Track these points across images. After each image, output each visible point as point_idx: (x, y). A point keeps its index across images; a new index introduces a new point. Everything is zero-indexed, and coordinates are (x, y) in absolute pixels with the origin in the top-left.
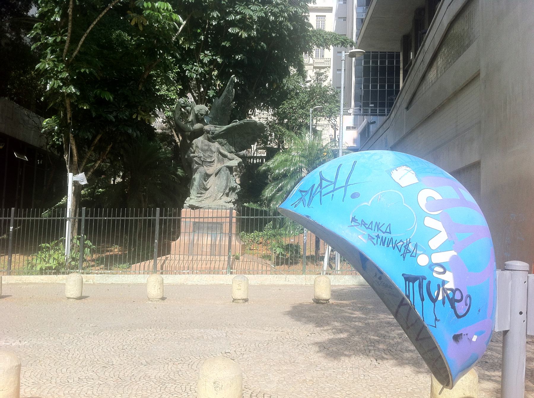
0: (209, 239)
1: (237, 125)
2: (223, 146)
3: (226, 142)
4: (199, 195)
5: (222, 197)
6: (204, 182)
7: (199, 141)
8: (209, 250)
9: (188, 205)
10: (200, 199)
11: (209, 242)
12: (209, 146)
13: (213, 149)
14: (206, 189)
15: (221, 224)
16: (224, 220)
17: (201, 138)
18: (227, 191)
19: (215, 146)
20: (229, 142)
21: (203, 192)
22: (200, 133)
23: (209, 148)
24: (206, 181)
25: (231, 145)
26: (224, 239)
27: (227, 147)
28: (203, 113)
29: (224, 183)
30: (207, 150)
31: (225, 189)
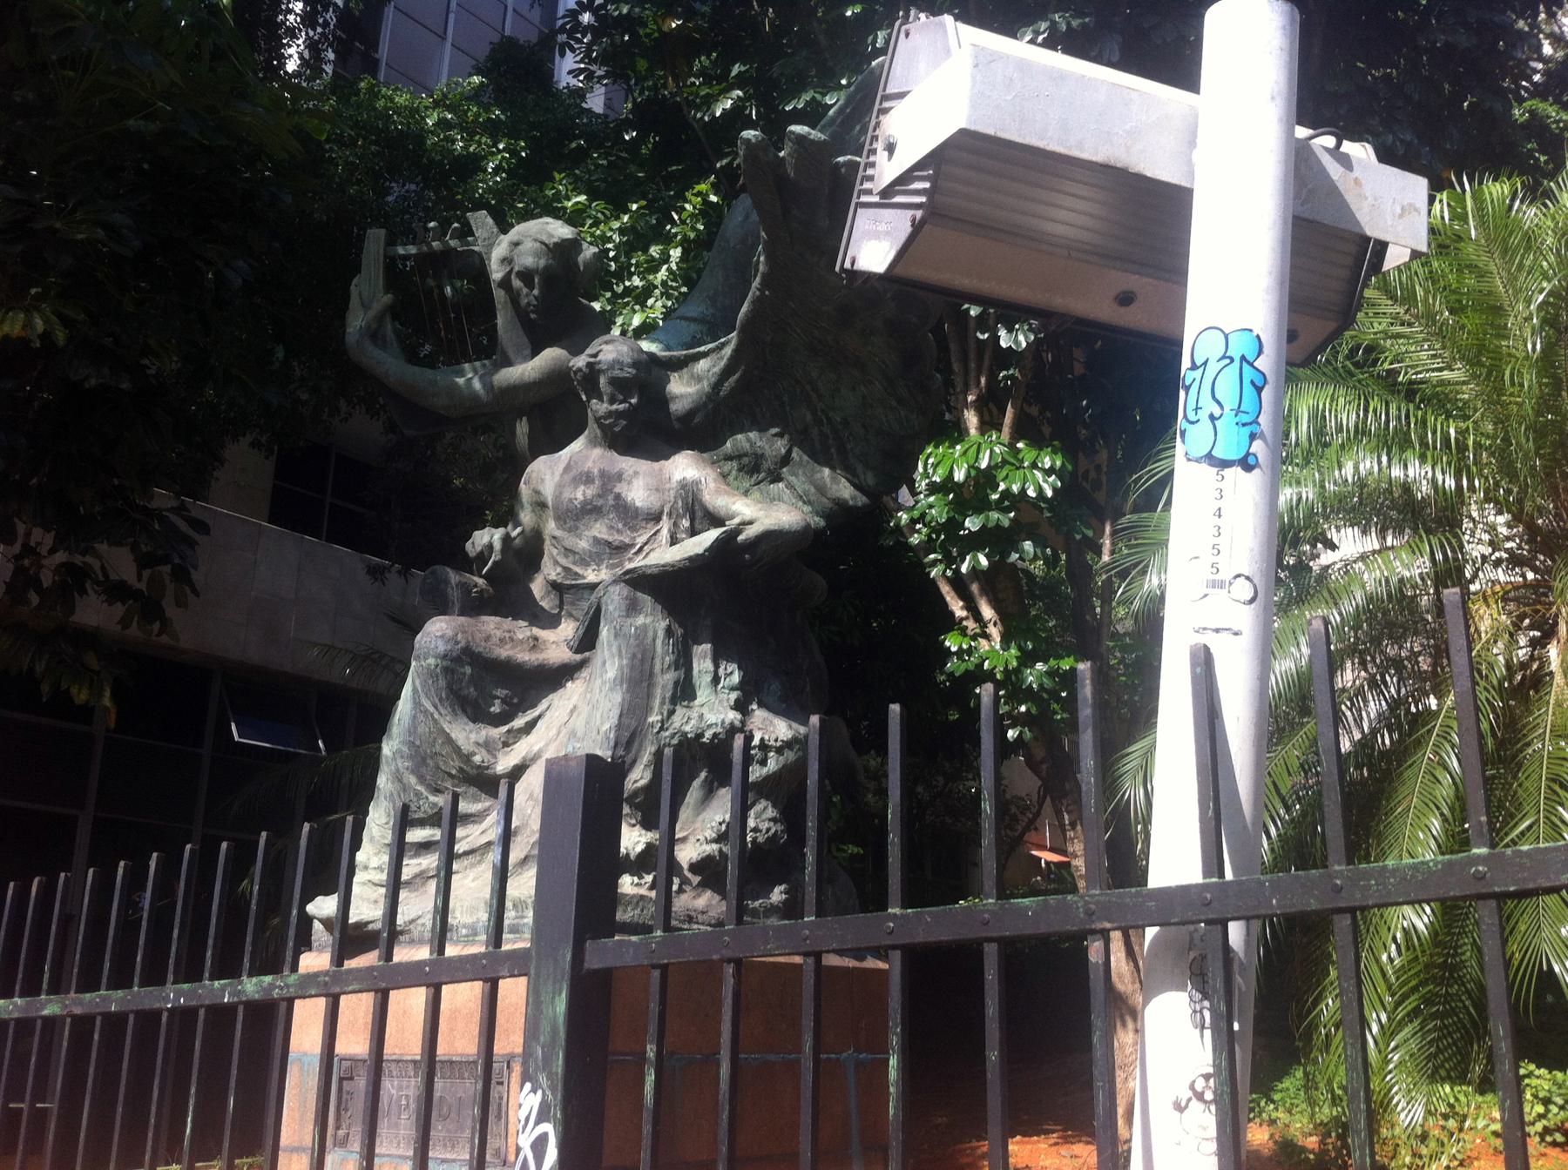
2: (777, 479)
3: (781, 446)
12: (609, 480)
13: (638, 494)
20: (800, 438)
22: (554, 414)
23: (605, 491)
25: (820, 456)
27: (800, 482)
30: (590, 510)
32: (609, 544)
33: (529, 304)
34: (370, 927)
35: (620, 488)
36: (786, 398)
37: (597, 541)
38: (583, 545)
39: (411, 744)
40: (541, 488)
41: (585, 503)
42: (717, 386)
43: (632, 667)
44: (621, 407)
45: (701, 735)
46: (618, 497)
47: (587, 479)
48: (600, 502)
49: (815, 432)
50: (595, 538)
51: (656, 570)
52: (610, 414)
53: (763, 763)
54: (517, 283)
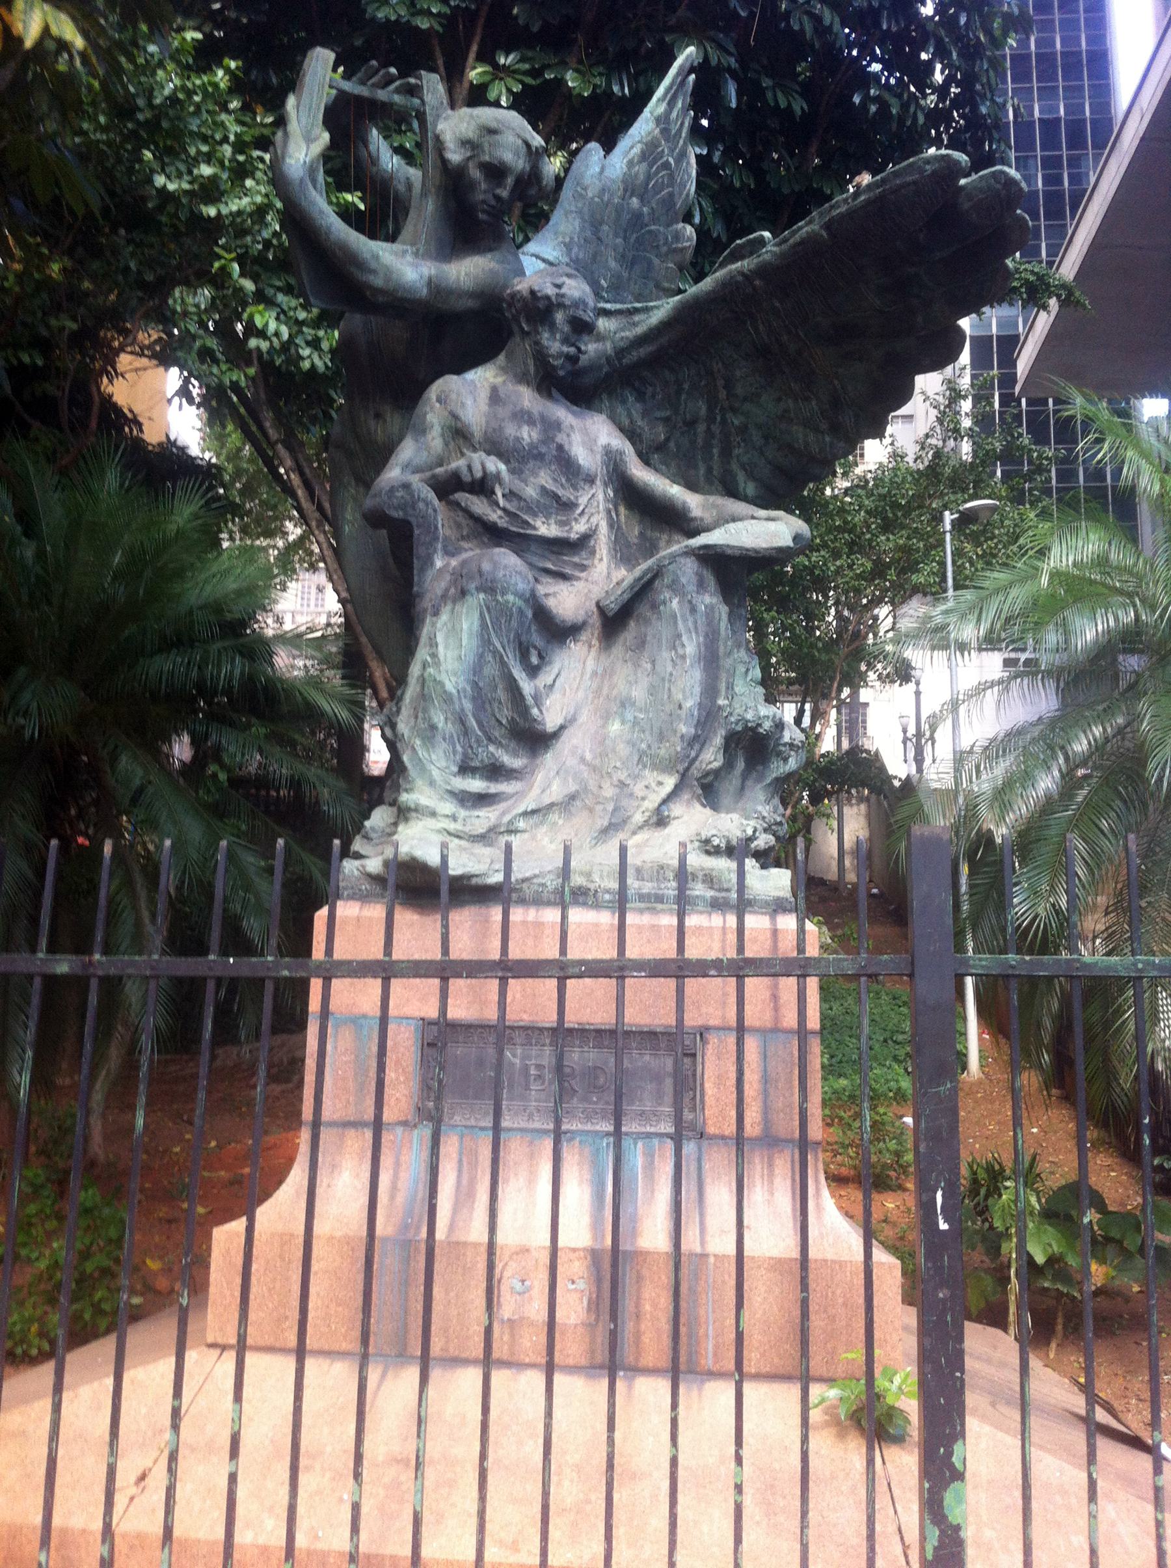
0: (577, 1194)
1: (763, 271)
4: (476, 785)
5: (676, 809)
6: (519, 674)
7: (473, 393)
8: (573, 1309)
9: (374, 865)
10: (484, 818)
11: (578, 1232)
12: (551, 427)
14: (534, 739)
15: (680, 1046)
16: (710, 1002)
17: (483, 377)
18: (711, 757)
19: (593, 437)
21: (507, 759)
23: (547, 439)
24: (533, 671)
26: (720, 1196)
28: (508, 157)
29: (688, 688)
31: (697, 741)
32: (556, 497)
33: (484, 202)
34: (474, 881)
35: (561, 438)
36: (686, 386)
37: (544, 491)
38: (530, 492)
39: (475, 685)
40: (461, 413)
41: (533, 446)
42: (620, 352)
43: (706, 646)
44: (572, 350)
45: (759, 725)
46: (560, 448)
47: (523, 417)
48: (543, 450)
49: (701, 428)
50: (543, 488)
51: (737, 553)
52: (560, 355)
53: (785, 760)
54: (475, 173)
